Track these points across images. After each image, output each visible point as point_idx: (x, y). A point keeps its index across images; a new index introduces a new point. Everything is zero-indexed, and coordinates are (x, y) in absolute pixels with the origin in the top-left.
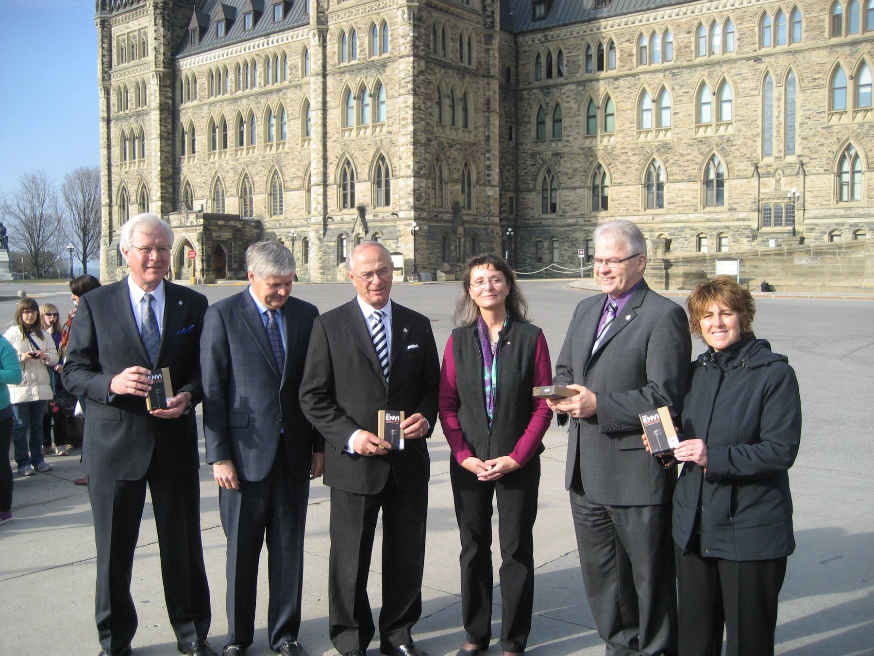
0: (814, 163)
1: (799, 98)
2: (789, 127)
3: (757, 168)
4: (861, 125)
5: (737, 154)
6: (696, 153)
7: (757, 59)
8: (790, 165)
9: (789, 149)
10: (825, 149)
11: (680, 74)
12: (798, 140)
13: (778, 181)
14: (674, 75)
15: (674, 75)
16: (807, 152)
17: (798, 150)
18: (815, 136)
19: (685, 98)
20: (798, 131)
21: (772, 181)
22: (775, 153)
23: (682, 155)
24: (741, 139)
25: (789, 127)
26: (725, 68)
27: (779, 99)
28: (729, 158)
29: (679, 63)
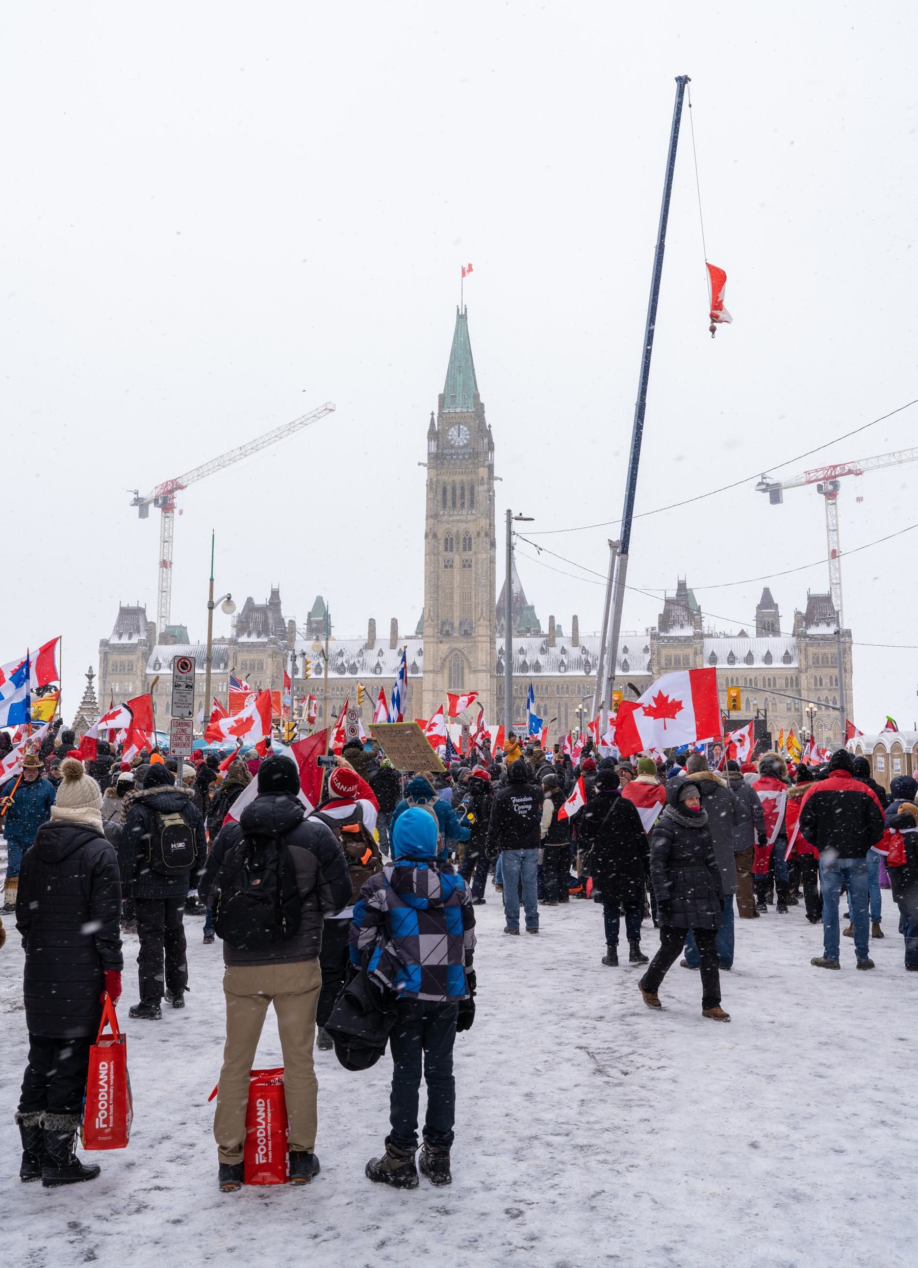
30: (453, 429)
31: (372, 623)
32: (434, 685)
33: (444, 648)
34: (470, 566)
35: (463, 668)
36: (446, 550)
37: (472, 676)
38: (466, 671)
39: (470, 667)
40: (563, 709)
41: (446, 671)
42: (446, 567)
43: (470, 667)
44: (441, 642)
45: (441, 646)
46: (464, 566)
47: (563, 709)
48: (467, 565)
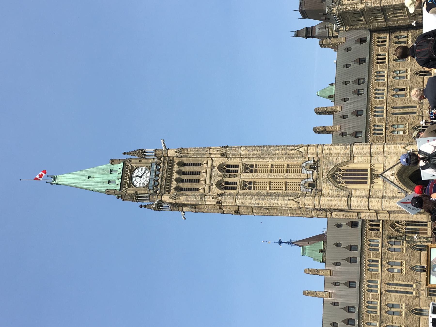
0: (416, 278)
1: (395, 282)
2: (404, 285)
3: (417, 297)
4: (406, 264)
5: (411, 303)
6: (410, 317)
7: (381, 293)
8: (416, 286)
9: (412, 286)
10: (413, 275)
11: (383, 320)
12: (409, 283)
13: (422, 290)
14: (382, 322)
15: (382, 322)
16: (413, 281)
17: (412, 283)
18: (408, 278)
19: (391, 319)
20: (406, 283)
21: (421, 292)
22: (412, 291)
23: (410, 322)
24: (407, 301)
25: (404, 285)
26: (383, 304)
27: (395, 288)
28: (413, 305)
29: (379, 320)
30: (135, 183)
31: (307, 293)
32: (363, 197)
33: (327, 188)
34: (252, 166)
35: (347, 170)
36: (235, 188)
37: (356, 161)
38: (351, 166)
39: (347, 163)
40: (398, 111)
41: (350, 186)
42: (250, 188)
43: (347, 163)
44: (321, 190)
45: (324, 191)
46: (251, 171)
47: (398, 111)
48: (249, 169)
